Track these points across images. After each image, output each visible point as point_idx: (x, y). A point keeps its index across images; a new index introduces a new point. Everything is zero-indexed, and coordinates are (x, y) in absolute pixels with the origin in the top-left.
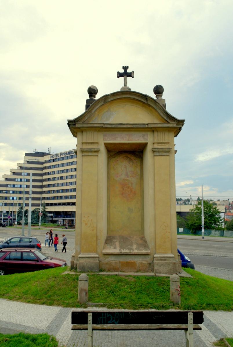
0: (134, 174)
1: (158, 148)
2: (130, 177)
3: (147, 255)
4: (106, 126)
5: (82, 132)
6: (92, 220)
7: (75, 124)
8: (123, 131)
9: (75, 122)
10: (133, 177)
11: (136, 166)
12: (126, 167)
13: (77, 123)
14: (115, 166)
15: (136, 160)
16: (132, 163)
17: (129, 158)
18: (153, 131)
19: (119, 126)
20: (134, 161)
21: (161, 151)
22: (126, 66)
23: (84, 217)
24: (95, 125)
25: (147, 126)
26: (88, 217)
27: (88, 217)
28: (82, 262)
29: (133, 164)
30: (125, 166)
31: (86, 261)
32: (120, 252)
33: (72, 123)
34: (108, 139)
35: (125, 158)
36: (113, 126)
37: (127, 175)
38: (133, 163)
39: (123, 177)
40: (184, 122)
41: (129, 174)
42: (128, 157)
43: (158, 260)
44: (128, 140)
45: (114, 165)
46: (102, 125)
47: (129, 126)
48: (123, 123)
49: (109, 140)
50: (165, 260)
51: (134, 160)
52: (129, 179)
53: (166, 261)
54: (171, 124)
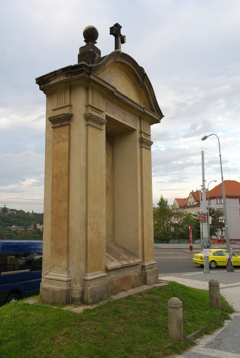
1: (146, 139)
3: (136, 265)
4: (116, 94)
5: (87, 89)
6: (97, 222)
7: (89, 74)
8: (122, 107)
9: (91, 70)
11: (109, 155)
13: (93, 73)
18: (140, 118)
19: (125, 99)
21: (147, 143)
22: (119, 25)
23: (90, 217)
24: (109, 87)
25: (142, 110)
26: (94, 217)
27: (94, 217)
28: (94, 286)
31: (96, 285)
32: (123, 265)
33: (86, 70)
34: (109, 111)
36: (120, 96)
40: (163, 118)
43: (148, 269)
44: (124, 120)
46: (114, 90)
47: (131, 104)
48: (129, 97)
49: (110, 113)
50: (152, 268)
53: (153, 269)
54: (156, 115)
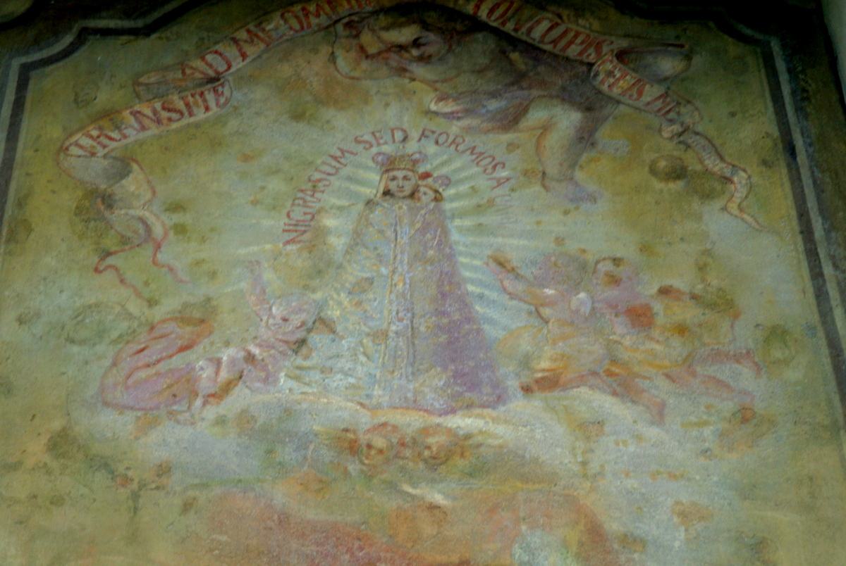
0: (640, 317)
2: (550, 383)
10: (621, 381)
11: (678, 173)
12: (407, 185)
14: (133, 184)
15: (668, 65)
16: (567, 120)
17: (481, 47)
20: (614, 79)
29: (585, 138)
30: (389, 165)
35: (406, 34)
37: (459, 353)
38: (593, 105)
39: (345, 389)
41: (499, 317)
42: (475, 25)
45: (123, 166)
51: (607, 65)
52: (514, 424)
